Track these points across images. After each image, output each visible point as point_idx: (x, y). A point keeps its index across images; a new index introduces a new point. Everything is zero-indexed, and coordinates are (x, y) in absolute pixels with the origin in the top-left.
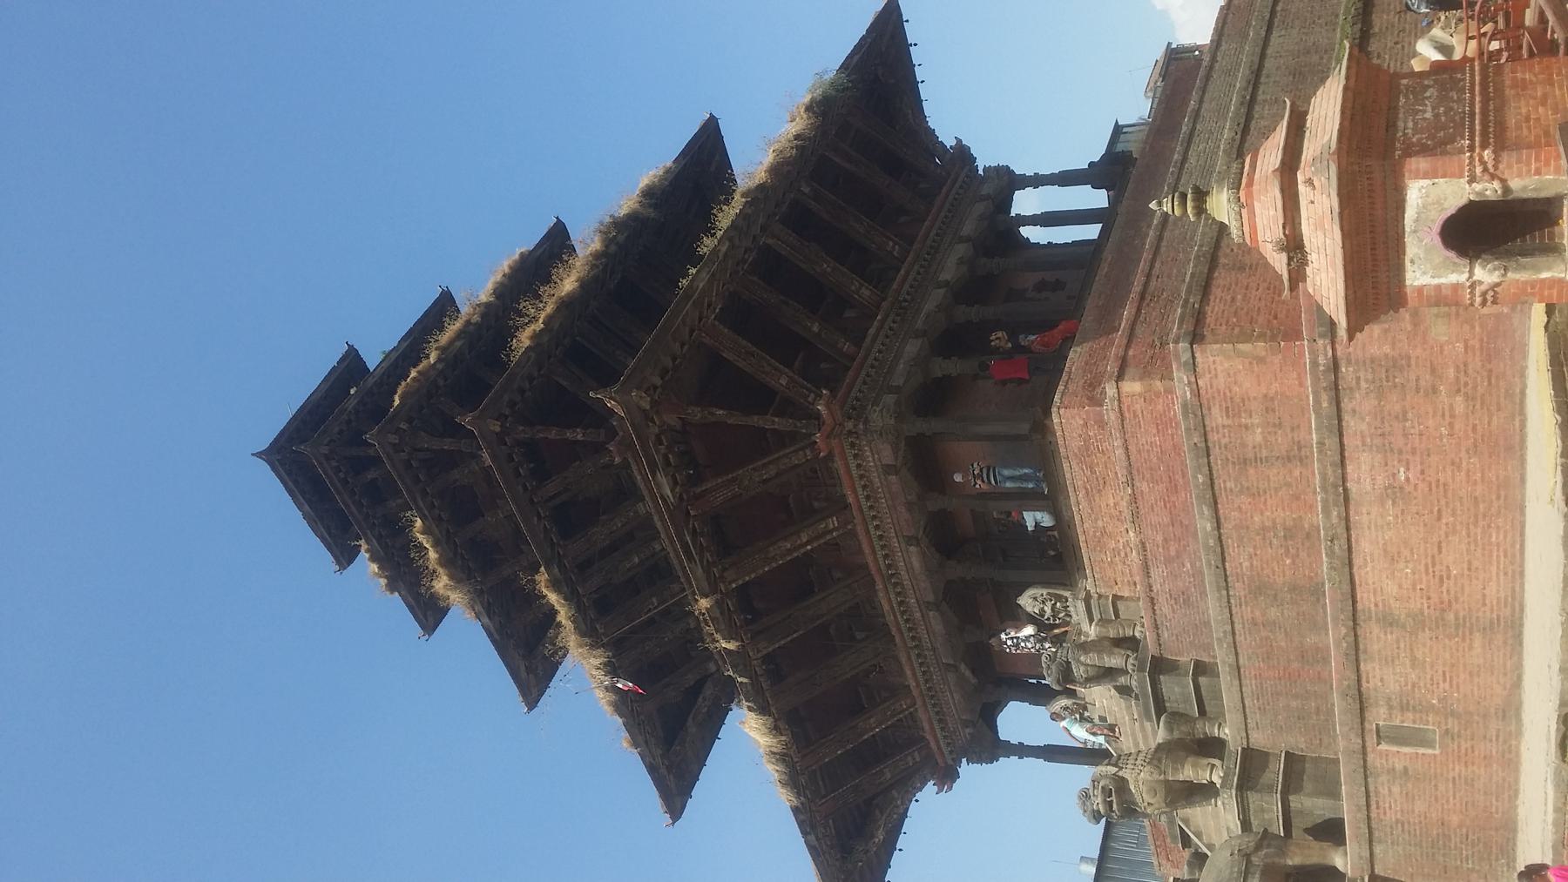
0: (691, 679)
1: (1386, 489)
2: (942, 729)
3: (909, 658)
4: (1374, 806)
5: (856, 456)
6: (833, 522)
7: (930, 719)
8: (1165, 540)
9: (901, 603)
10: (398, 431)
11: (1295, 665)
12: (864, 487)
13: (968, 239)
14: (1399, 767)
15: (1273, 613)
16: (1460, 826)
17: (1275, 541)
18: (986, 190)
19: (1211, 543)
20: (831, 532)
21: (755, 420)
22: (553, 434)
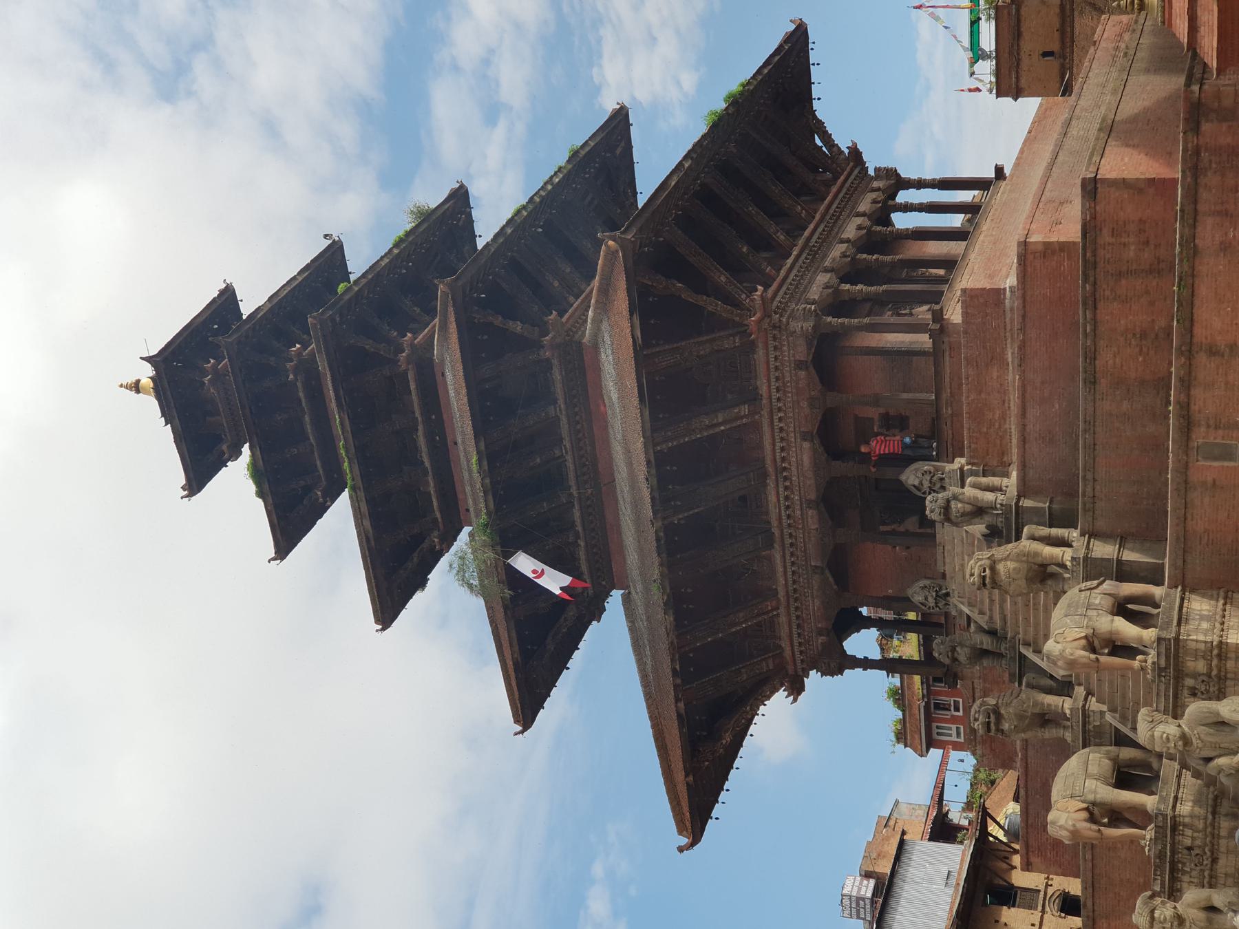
1: (1221, 243)
2: (799, 634)
3: (784, 556)
5: (775, 348)
6: (745, 409)
8: (1043, 383)
9: (787, 498)
12: (777, 379)
13: (863, 214)
14: (1210, 479)
15: (1125, 406)
17: (1133, 342)
18: (875, 184)
20: (742, 418)
21: (703, 300)
22: (498, 321)
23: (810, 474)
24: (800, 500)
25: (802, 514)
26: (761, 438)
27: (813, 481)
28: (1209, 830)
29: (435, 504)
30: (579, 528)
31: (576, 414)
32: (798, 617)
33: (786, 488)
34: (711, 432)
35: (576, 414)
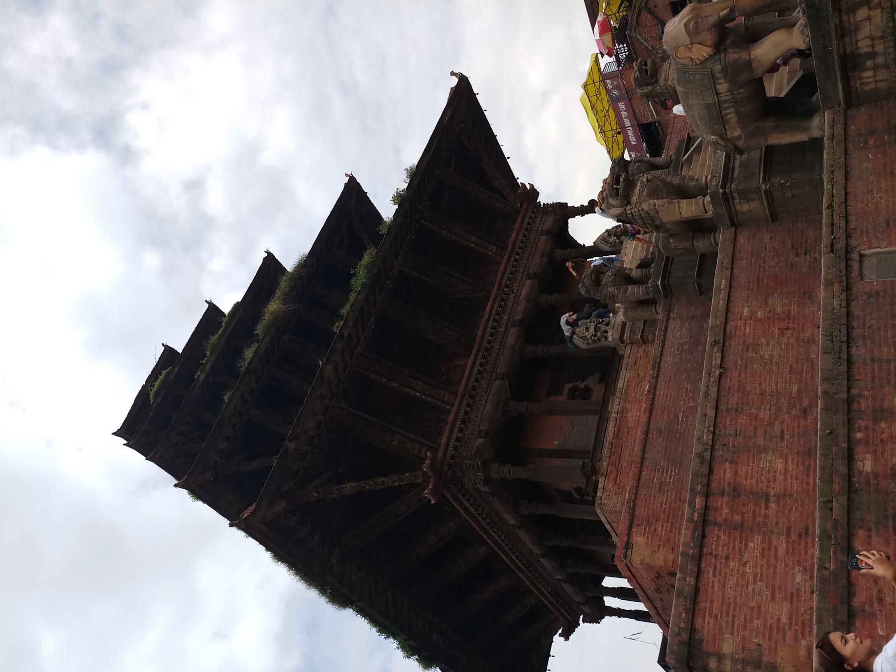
2: (461, 430)
5: (531, 218)
7: (457, 414)
9: (498, 313)
24: (508, 321)
32: (466, 413)
33: (500, 306)
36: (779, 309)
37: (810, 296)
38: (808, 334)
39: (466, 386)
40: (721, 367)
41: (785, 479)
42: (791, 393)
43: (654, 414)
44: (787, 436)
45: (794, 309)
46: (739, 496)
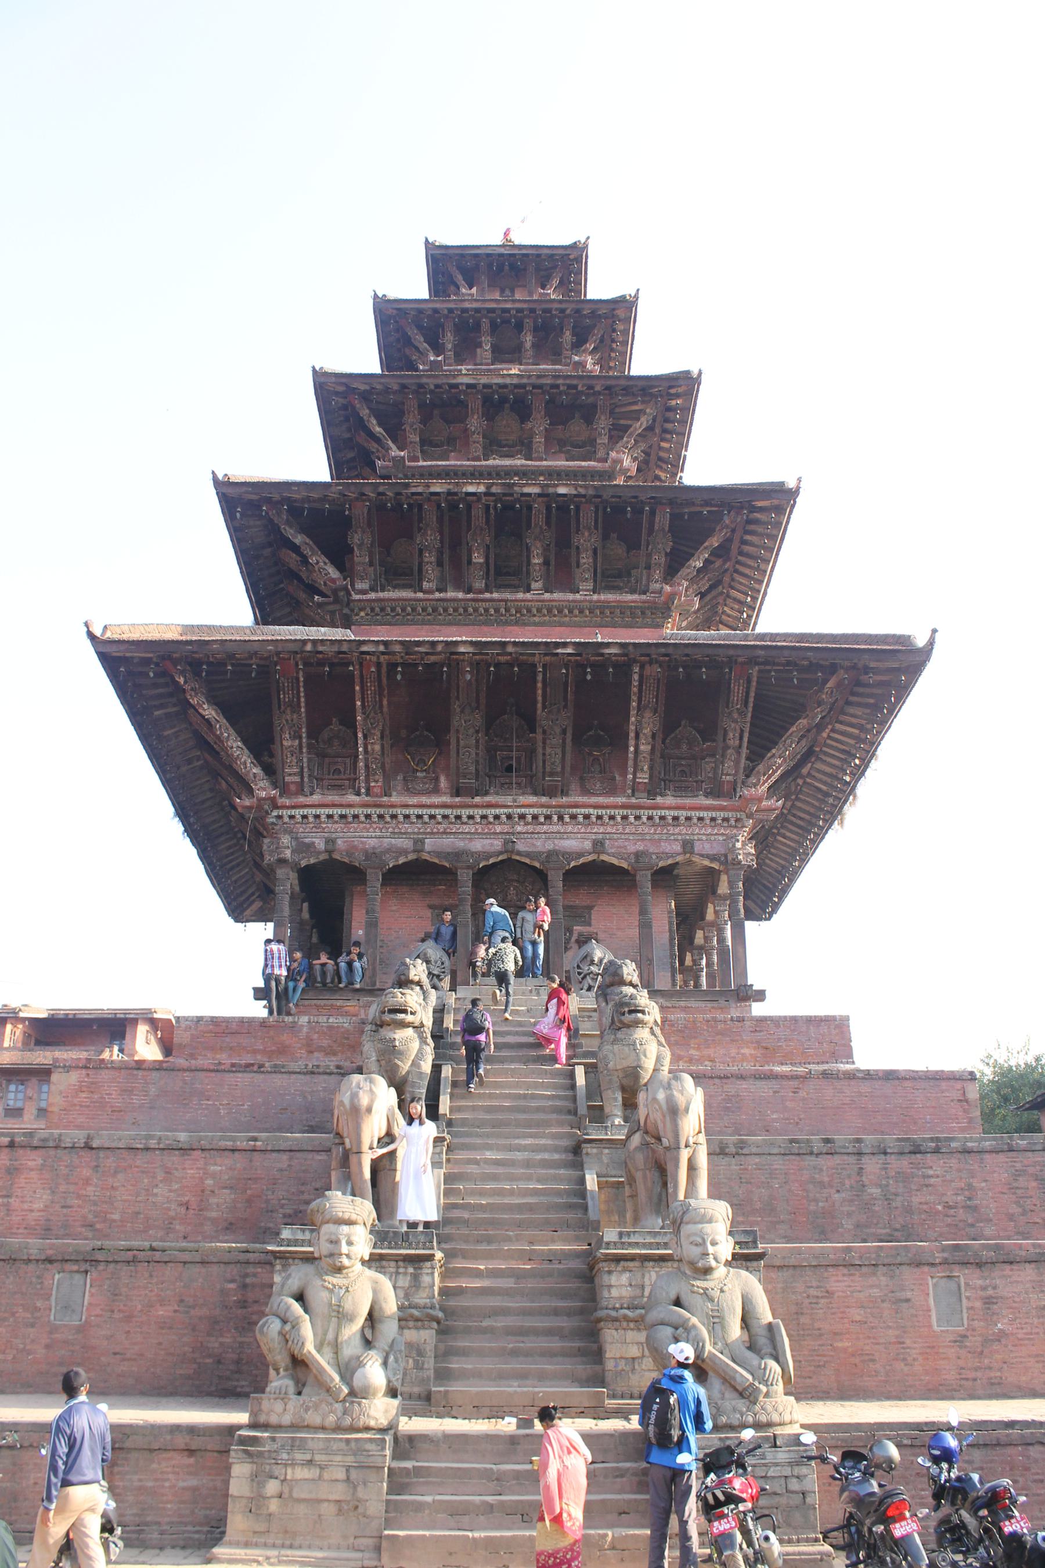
0: (360, 558)
2: (330, 817)
4: (845, 1271)
5: (713, 819)
6: (643, 778)
7: (350, 806)
8: (804, 1099)
9: (522, 817)
10: (678, 396)
11: (812, 1208)
14: (909, 1295)
16: (835, 1349)
19: (954, 1145)
20: (634, 774)
23: (551, 847)
25: (495, 833)
26: (594, 794)
27: (540, 849)
28: (416, 1312)
29: (440, 463)
30: (437, 595)
31: (581, 611)
32: (356, 817)
33: (535, 817)
34: (632, 735)
35: (581, 611)
36: (213, 1200)
37: (227, 1229)
38: (177, 1227)
39: (393, 806)
40: (147, 1149)
41: (22, 1210)
42: (112, 1213)
43: (213, 1074)
44: (65, 1210)
45: (214, 1214)
46: (10, 1173)
